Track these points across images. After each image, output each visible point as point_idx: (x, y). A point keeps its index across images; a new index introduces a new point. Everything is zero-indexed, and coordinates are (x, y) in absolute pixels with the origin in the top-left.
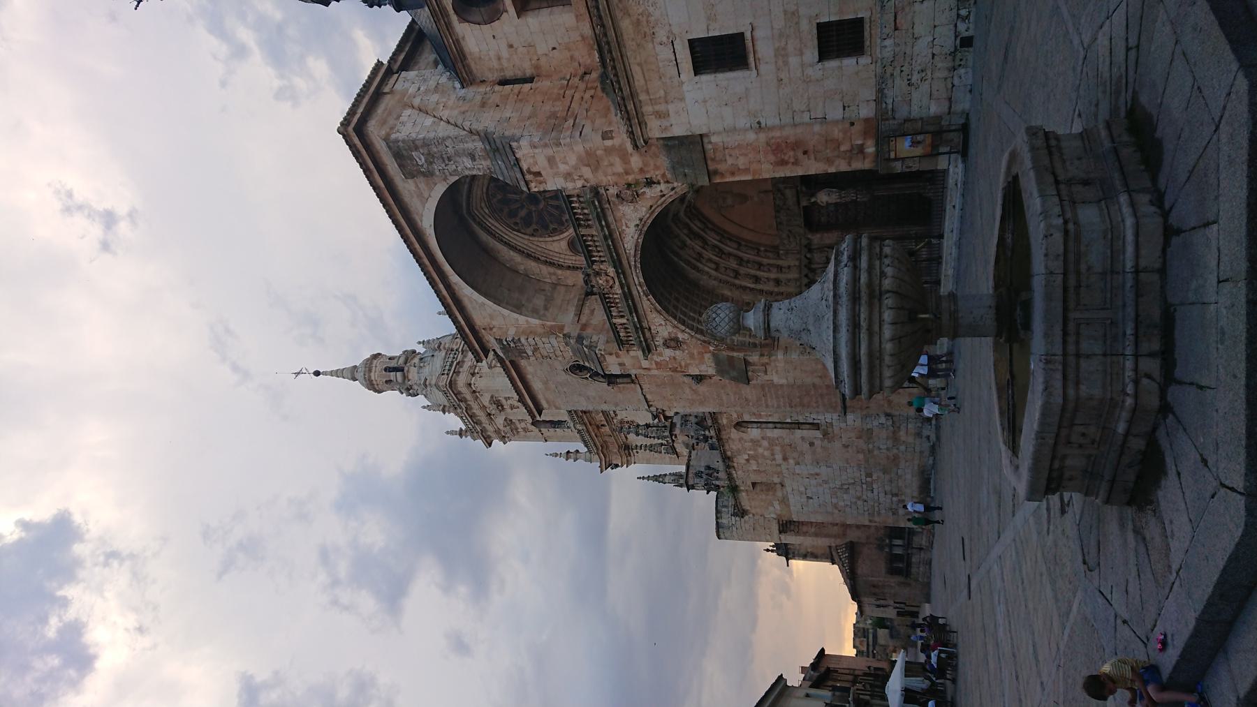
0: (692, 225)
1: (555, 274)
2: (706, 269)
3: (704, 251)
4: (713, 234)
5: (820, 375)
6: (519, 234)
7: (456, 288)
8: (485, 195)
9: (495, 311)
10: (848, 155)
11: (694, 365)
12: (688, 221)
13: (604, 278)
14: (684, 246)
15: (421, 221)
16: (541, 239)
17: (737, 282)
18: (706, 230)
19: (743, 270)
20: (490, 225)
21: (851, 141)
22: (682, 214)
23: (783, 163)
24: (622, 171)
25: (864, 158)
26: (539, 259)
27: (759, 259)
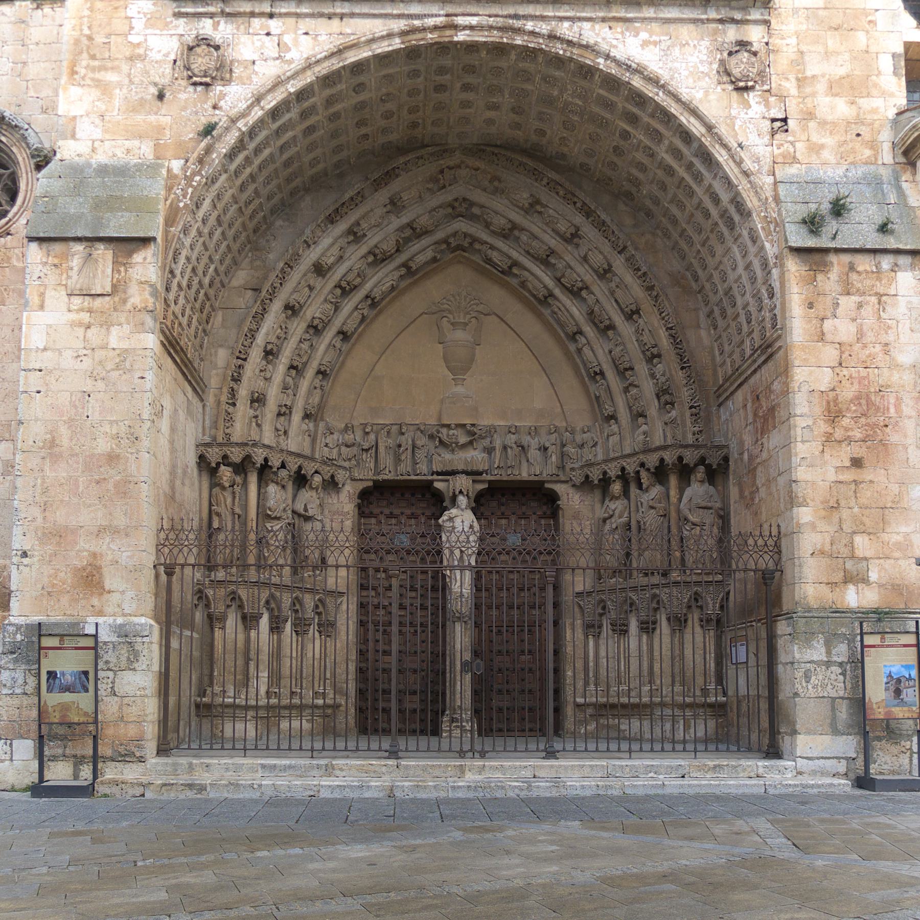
0: (426, 241)
2: (326, 242)
3: (364, 250)
5: (65, 442)
10: (842, 550)
11: (102, 106)
12: (440, 235)
14: (395, 205)
17: (276, 307)
18: (403, 271)
19: (298, 328)
22: (461, 225)
23: (833, 413)
24: (809, 73)
25: (832, 585)
27: (310, 373)
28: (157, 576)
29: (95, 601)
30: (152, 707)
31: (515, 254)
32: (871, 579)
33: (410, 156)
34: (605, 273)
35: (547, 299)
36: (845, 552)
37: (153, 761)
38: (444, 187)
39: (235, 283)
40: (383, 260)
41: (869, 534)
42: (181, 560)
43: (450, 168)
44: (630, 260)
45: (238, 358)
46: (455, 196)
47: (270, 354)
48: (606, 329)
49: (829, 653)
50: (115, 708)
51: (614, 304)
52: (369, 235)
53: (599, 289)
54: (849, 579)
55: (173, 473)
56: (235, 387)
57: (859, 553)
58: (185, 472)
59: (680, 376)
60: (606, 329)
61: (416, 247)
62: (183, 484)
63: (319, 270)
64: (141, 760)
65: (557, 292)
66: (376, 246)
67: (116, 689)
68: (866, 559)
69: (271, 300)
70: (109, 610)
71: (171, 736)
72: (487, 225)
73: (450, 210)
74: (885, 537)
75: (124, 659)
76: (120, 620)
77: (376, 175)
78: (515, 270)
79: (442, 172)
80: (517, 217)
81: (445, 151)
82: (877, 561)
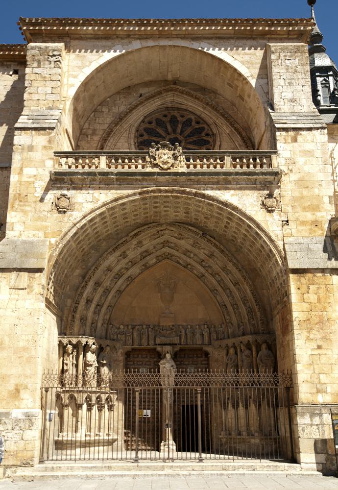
1: (94, 133)
4: (138, 271)
6: (140, 121)
7: (123, 41)
8: (184, 107)
9: (91, 62)
10: (315, 380)
12: (158, 253)
13: (171, 161)
15: (208, 43)
16: (133, 136)
17: (91, 284)
19: (100, 290)
20: (155, 101)
21: (331, 383)
26: (116, 126)
28: (42, 392)
29: (17, 403)
30: (38, 444)
31: (188, 260)
32: (328, 392)
33: (146, 227)
34: (224, 269)
35: (201, 277)
36: (316, 381)
37: (37, 466)
38: (159, 237)
39: (75, 274)
40: (136, 263)
41: (326, 374)
42: (51, 385)
43: (161, 230)
44: (234, 264)
45: (76, 303)
46: (164, 240)
47: (89, 301)
48: (225, 288)
49: (311, 420)
50: (23, 445)
51: (229, 280)
52: (130, 255)
53: (223, 274)
54: (318, 391)
55: (48, 351)
56: (74, 314)
57: (322, 381)
58: (53, 349)
59: (256, 308)
60: (225, 288)
61: (148, 258)
62: (52, 354)
63: (109, 269)
64: (32, 466)
65: (206, 275)
66: (133, 259)
67: (23, 438)
68: (325, 383)
69: (89, 281)
70: (22, 406)
71: (45, 455)
72: (178, 251)
73: (162, 245)
74: (333, 375)
75: (27, 425)
76: (26, 410)
77: (133, 233)
78: (189, 267)
79: (158, 232)
80: (189, 248)
81: (160, 225)
82: (330, 385)
